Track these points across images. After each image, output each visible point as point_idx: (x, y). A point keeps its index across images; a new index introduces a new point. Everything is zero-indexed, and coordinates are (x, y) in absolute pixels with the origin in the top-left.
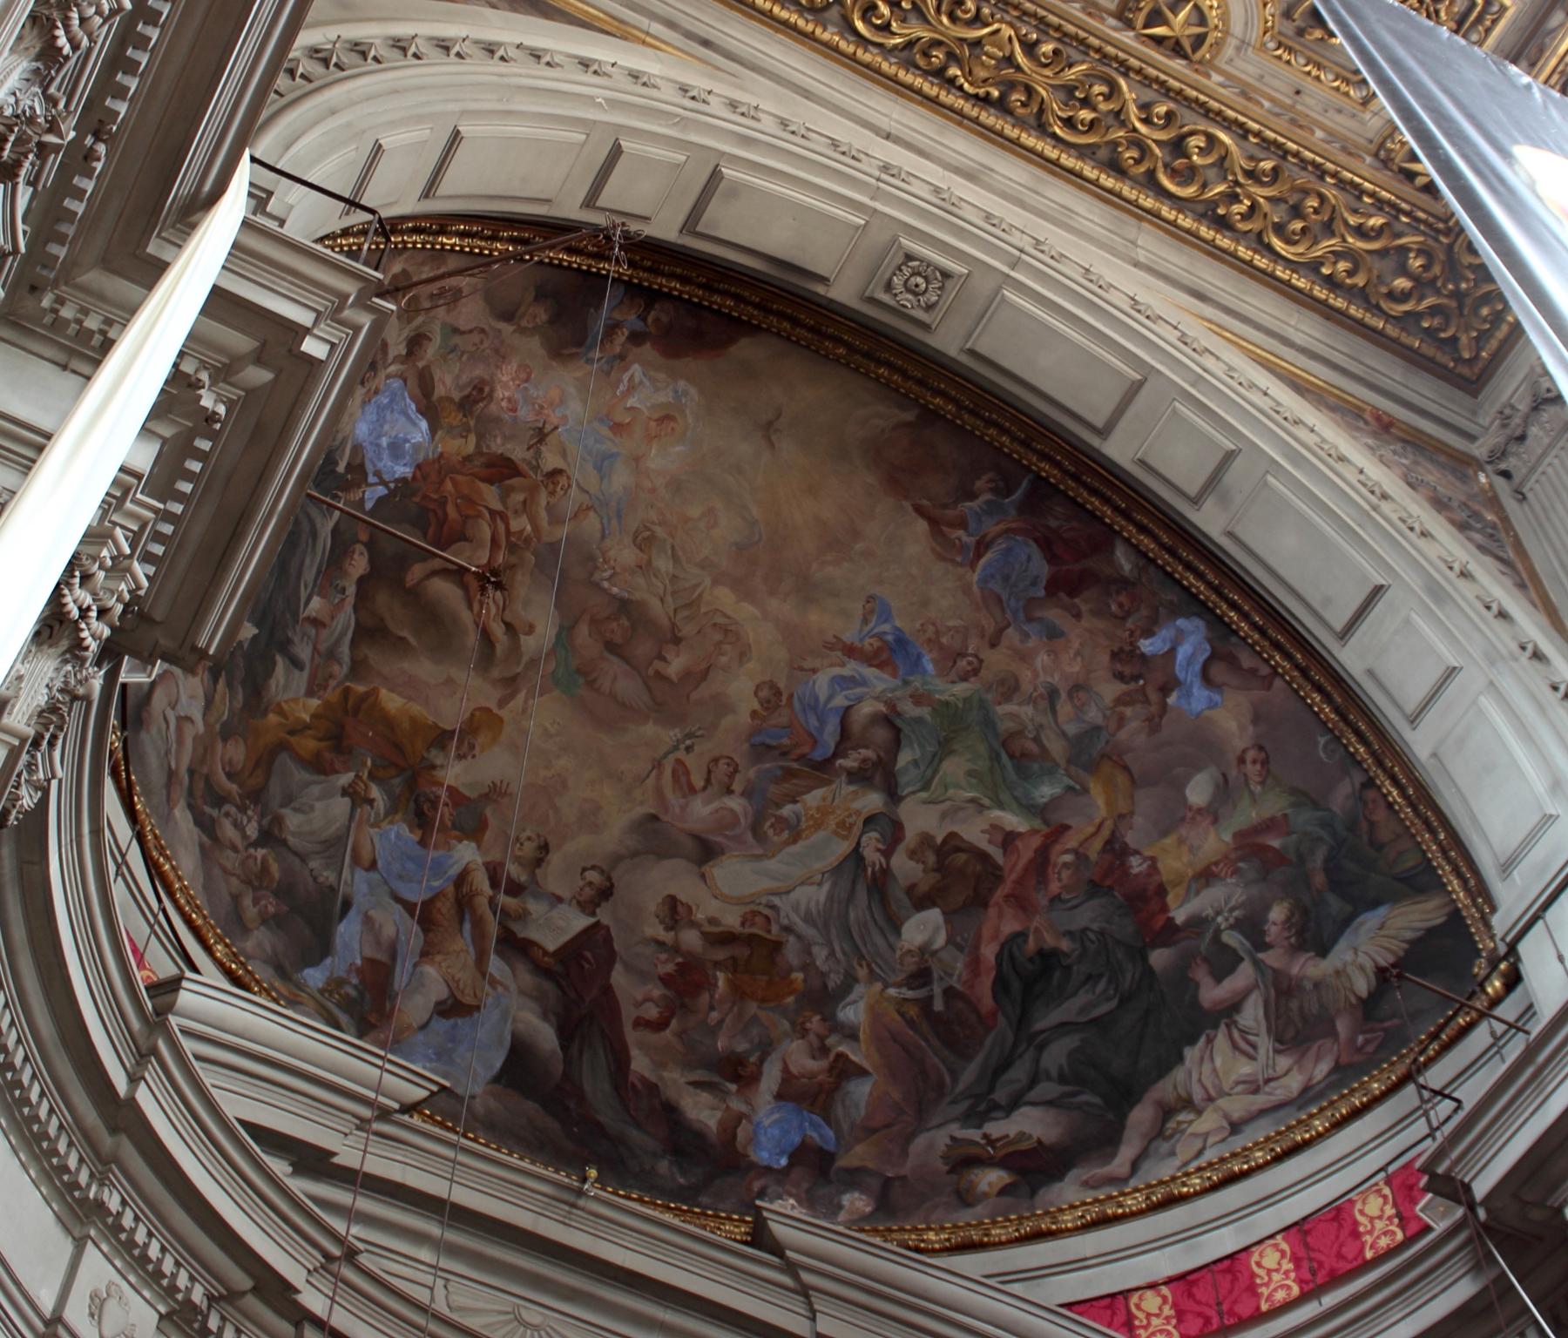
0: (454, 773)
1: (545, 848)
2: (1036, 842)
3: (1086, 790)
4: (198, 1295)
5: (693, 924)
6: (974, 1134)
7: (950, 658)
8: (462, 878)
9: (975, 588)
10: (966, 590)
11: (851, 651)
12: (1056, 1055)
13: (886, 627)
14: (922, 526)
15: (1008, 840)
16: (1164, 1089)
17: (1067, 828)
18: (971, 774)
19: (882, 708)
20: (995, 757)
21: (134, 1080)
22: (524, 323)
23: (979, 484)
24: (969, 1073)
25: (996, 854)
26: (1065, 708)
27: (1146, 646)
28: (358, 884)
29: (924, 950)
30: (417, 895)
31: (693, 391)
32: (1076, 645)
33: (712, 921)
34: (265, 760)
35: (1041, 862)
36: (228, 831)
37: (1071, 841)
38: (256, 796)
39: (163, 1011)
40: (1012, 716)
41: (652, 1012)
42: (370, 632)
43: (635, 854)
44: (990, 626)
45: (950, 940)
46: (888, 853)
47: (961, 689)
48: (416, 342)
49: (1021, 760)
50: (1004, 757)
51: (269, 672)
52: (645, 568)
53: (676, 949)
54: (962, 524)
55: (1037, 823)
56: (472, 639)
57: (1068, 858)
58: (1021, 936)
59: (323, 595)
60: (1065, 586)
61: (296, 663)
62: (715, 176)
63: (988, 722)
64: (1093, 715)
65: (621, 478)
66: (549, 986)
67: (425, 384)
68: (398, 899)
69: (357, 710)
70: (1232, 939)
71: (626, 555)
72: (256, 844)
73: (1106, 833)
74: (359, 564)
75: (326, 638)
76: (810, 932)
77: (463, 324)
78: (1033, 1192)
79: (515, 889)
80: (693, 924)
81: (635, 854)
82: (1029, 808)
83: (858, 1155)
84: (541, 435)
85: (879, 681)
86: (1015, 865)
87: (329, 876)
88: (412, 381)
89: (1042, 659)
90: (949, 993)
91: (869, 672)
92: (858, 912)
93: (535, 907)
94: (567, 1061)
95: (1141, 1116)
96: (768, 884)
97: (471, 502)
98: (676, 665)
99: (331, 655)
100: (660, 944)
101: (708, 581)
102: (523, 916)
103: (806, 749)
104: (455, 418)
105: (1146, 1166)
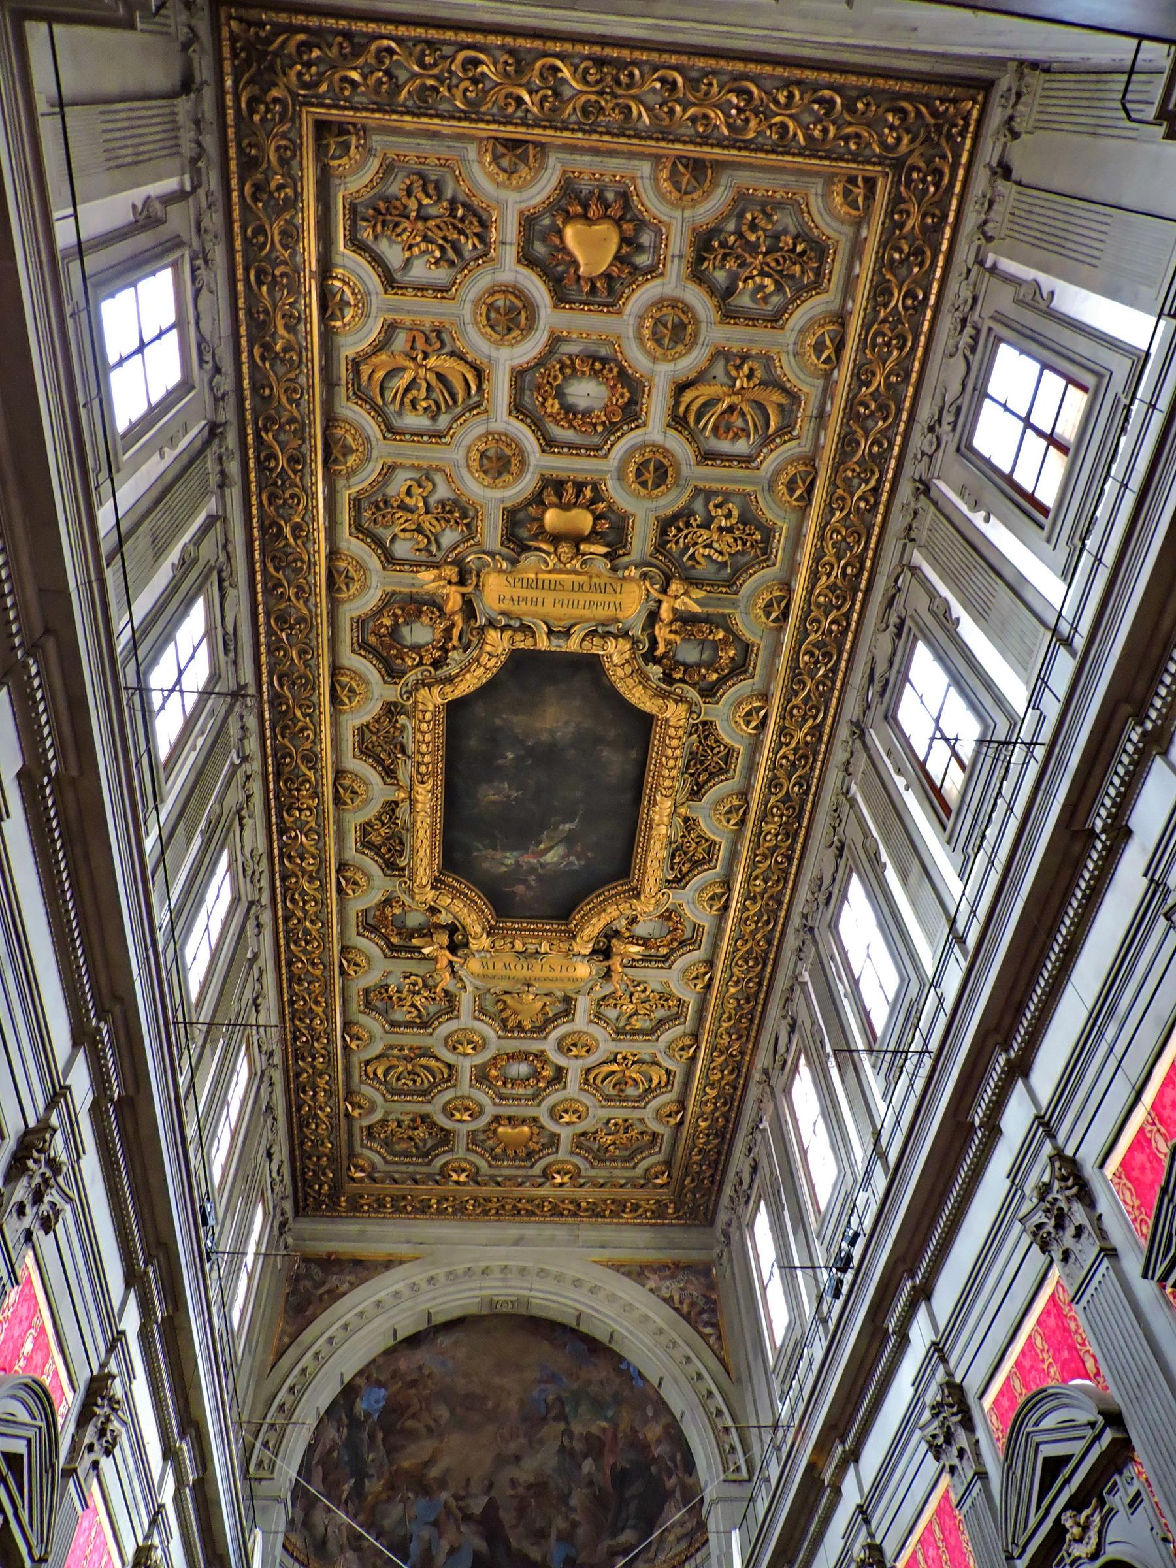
0: (434, 1472)
1: (468, 1480)
6: (612, 1542)
12: (633, 1507)
15: (604, 1430)
24: (610, 1516)
28: (412, 1528)
30: (432, 1519)
37: (622, 1427)
42: (392, 1450)
56: (424, 1431)
58: (614, 1464)
71: (462, 1382)
74: (380, 1435)
79: (463, 1498)
82: (606, 1419)
84: (420, 1368)
86: (608, 1439)
87: (402, 1532)
93: (471, 1501)
98: (490, 1404)
99: (381, 1465)
102: (468, 1506)
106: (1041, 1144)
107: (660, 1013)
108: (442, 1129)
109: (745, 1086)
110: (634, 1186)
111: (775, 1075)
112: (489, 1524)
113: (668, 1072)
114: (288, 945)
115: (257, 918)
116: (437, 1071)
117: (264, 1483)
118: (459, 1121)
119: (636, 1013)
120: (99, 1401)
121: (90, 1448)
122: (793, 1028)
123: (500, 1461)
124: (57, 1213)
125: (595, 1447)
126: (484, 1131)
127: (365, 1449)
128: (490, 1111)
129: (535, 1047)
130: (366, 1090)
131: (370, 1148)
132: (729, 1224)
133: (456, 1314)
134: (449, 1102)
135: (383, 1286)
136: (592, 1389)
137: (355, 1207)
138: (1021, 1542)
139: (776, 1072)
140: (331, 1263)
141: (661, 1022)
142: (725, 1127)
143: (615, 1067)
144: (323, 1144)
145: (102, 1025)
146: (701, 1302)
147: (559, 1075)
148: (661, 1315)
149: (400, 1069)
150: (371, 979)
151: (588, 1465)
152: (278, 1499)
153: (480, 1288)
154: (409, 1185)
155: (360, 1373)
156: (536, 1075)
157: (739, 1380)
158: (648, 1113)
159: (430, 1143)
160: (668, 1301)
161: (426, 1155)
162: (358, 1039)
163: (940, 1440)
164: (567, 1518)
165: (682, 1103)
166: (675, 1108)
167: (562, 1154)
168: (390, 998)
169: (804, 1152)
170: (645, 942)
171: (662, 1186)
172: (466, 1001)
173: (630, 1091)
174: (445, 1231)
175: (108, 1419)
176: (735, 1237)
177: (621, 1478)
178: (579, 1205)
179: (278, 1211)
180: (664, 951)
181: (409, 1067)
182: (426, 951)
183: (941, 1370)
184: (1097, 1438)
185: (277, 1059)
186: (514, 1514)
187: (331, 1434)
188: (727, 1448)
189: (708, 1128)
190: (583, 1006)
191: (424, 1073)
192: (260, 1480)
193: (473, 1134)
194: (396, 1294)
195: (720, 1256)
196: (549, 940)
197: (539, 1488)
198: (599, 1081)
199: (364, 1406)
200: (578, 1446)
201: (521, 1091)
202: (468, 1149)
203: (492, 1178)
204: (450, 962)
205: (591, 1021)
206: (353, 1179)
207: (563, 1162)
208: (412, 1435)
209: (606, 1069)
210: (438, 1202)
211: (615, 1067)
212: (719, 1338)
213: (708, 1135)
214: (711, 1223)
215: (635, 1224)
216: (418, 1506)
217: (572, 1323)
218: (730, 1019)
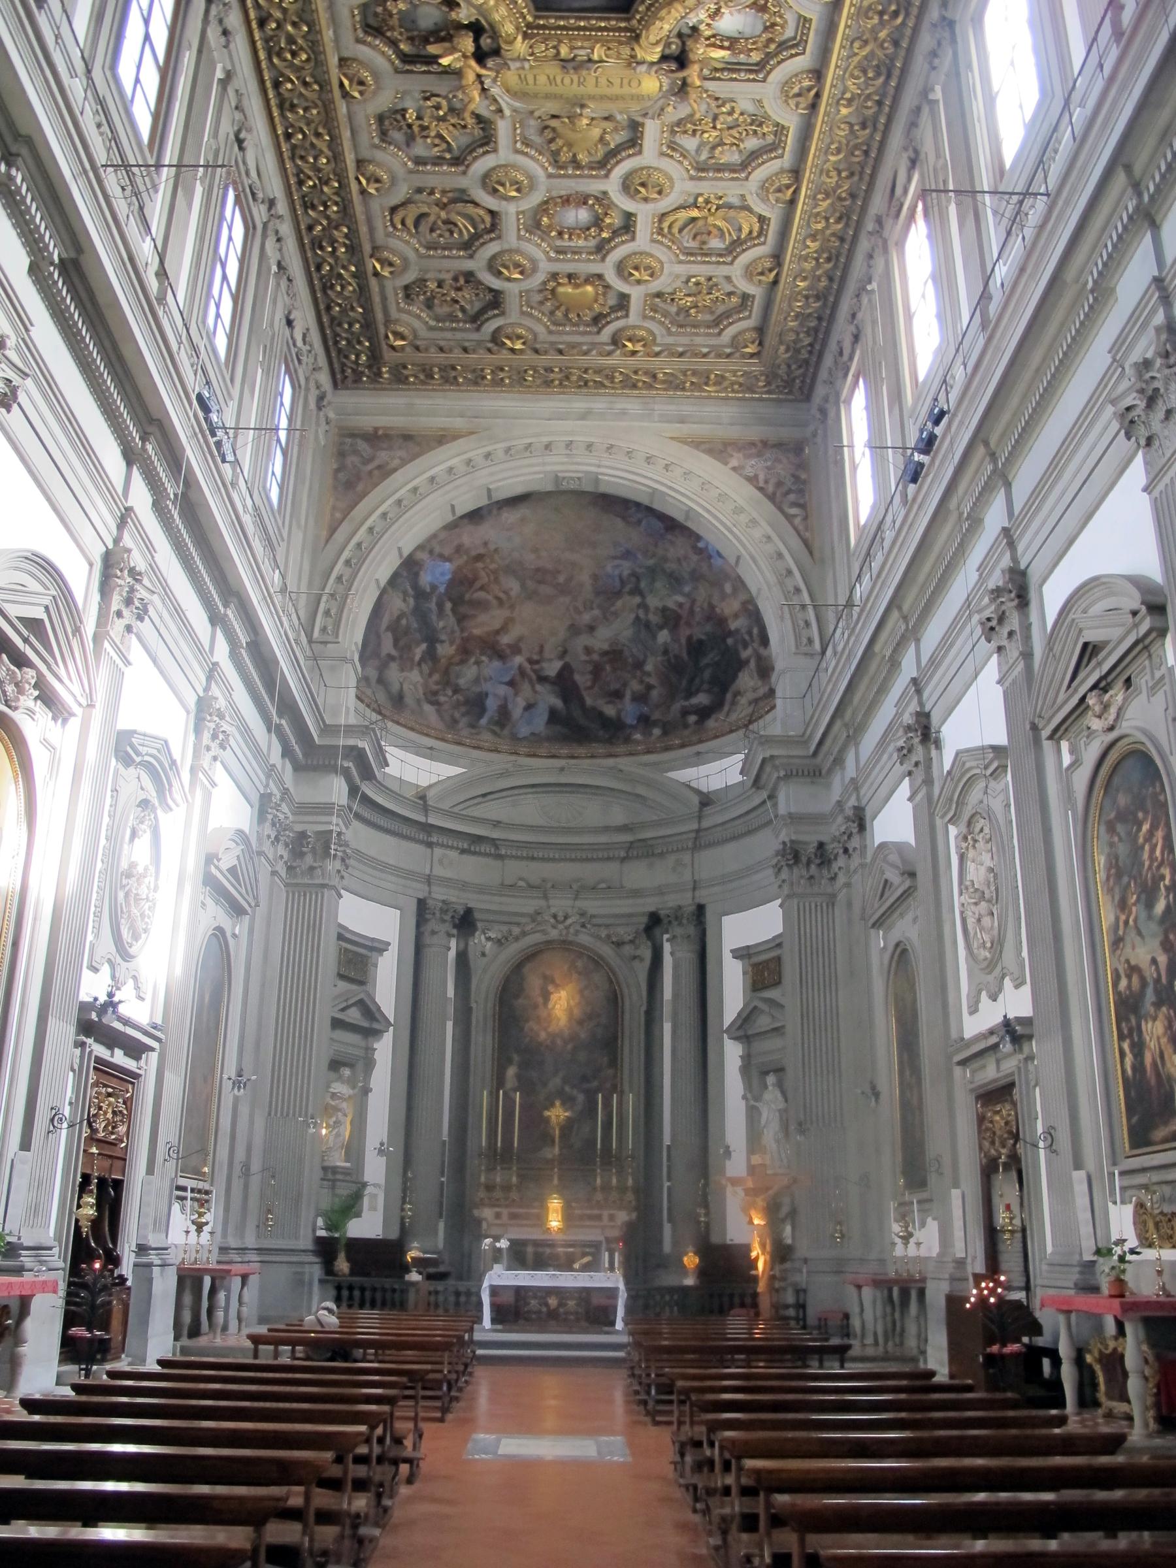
0: (505, 640)
1: (542, 647)
4: (466, 846)
6: (686, 703)
8: (520, 667)
11: (615, 558)
12: (707, 674)
15: (681, 605)
21: (426, 816)
24: (684, 683)
26: (684, 564)
28: (487, 687)
29: (665, 643)
30: (507, 679)
34: (446, 672)
35: (692, 612)
36: (442, 699)
37: (698, 604)
39: (425, 802)
41: (589, 684)
42: (461, 619)
48: (431, 552)
51: (435, 649)
56: (495, 602)
61: (442, 642)
62: (489, 490)
70: (747, 637)
71: (532, 556)
74: (448, 605)
79: (537, 662)
83: (656, 716)
84: (486, 544)
87: (478, 690)
90: (676, 657)
93: (545, 665)
95: (729, 696)
98: (561, 579)
99: (453, 632)
100: (586, 662)
102: (542, 669)
106: (1153, 311)
107: (751, 143)
108: (491, 290)
109: (855, 237)
110: (719, 356)
111: (887, 224)
112: (564, 683)
113: (762, 219)
114: (270, 59)
115: (221, 21)
116: (478, 219)
117: (329, 646)
118: (509, 279)
119: (722, 144)
120: (119, 573)
121: (119, 614)
122: (913, 162)
123: (574, 630)
124: (14, 390)
125: (671, 619)
126: (540, 291)
127: (434, 617)
128: (545, 267)
129: (594, 186)
130: (394, 243)
131: (409, 313)
132: (826, 400)
133: (519, 490)
134: (494, 258)
135: (439, 461)
136: (670, 566)
137: (399, 378)
138: (1047, 716)
139: (891, 221)
140: (376, 438)
141: (754, 155)
142: (828, 288)
143: (695, 213)
144: (353, 309)
145: (13, 172)
146: (789, 483)
147: (628, 225)
148: (742, 493)
149: (432, 218)
150: (383, 101)
151: (664, 636)
152: (344, 659)
153: (544, 464)
154: (457, 354)
155: (420, 547)
156: (597, 222)
158: (736, 271)
159: (478, 306)
160: (753, 480)
161: (477, 319)
162: (378, 181)
163: (994, 623)
164: (642, 682)
165: (777, 257)
166: (768, 265)
167: (634, 318)
168: (410, 126)
169: (909, 317)
170: (732, 43)
171: (752, 356)
172: (503, 129)
173: (715, 243)
174: (502, 403)
175: (132, 590)
176: (832, 414)
177: (696, 648)
178: (654, 376)
179: (312, 385)
180: (756, 57)
181: (443, 215)
182: (445, 61)
183: (1008, 555)
184: (1136, 625)
185: (282, 207)
186: (589, 677)
187: (398, 604)
188: (802, 624)
189: (808, 288)
190: (652, 131)
191: (460, 221)
192: (325, 643)
193: (525, 294)
194: (450, 470)
195: (815, 435)
196: (604, 42)
197: (614, 655)
198: (675, 230)
200: (654, 619)
201: (581, 243)
202: (523, 313)
203: (552, 343)
204: (479, 76)
205: (663, 154)
206: (393, 348)
207: (634, 327)
209: (683, 215)
210: (492, 372)
211: (695, 213)
212: (805, 518)
213: (807, 297)
214: (808, 398)
215: (718, 398)
216: (492, 667)
217: (645, 501)
218: (839, 151)
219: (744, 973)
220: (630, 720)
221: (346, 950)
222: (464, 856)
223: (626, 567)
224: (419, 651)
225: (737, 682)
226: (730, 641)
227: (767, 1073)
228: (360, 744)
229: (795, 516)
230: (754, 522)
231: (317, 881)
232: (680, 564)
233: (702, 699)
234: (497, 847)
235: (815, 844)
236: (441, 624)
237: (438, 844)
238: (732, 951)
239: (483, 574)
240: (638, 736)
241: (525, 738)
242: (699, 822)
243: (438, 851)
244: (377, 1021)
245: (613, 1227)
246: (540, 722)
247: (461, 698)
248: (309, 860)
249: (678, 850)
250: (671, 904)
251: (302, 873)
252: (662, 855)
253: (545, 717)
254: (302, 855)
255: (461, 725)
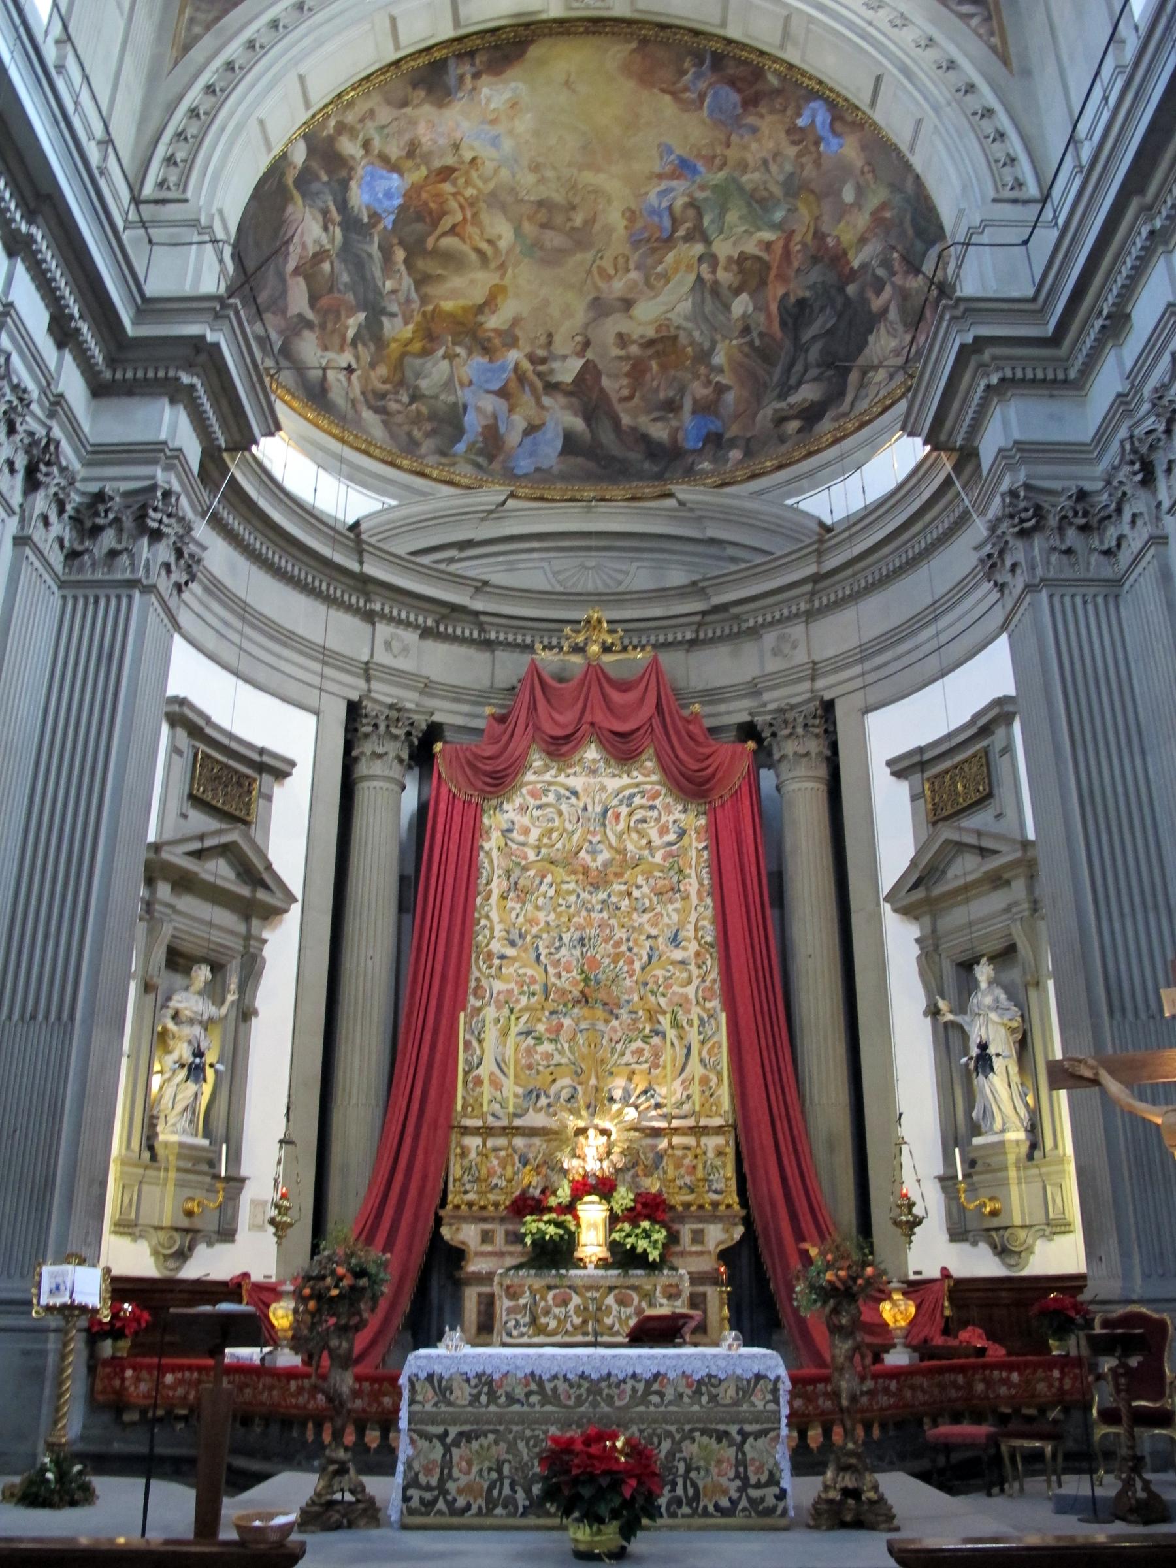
0: (494, 322)
2: (781, 243)
3: (796, 210)
5: (634, 342)
6: (783, 405)
7: (710, 160)
8: (516, 368)
9: (708, 121)
10: (703, 122)
11: (660, 177)
12: (814, 354)
13: (672, 157)
14: (667, 98)
15: (768, 246)
16: (861, 361)
17: (793, 232)
18: (740, 218)
19: (686, 199)
20: (749, 205)
22: (415, 102)
23: (686, 65)
24: (778, 372)
25: (764, 255)
26: (774, 168)
27: (801, 122)
28: (464, 395)
29: (744, 316)
30: (496, 386)
31: (521, 85)
32: (767, 132)
33: (642, 337)
36: (393, 406)
37: (797, 238)
38: (401, 383)
40: (751, 181)
41: (625, 392)
42: (422, 281)
43: (594, 320)
44: (723, 137)
45: (755, 308)
46: (714, 272)
47: (721, 175)
48: (366, 145)
49: (762, 202)
50: (755, 205)
51: (381, 324)
52: (542, 180)
53: (627, 358)
54: (686, 89)
55: (779, 233)
56: (473, 256)
57: (798, 247)
58: (786, 295)
59: (389, 278)
60: (751, 102)
61: (393, 315)
63: (741, 189)
64: (788, 168)
65: (507, 144)
66: (574, 400)
67: (384, 159)
68: (489, 392)
69: (433, 318)
70: (880, 272)
71: (531, 179)
72: (411, 403)
73: (812, 230)
74: (400, 254)
75: (401, 297)
76: (689, 325)
77: (384, 122)
78: (811, 430)
79: (543, 361)
80: (634, 342)
81: (594, 320)
82: (774, 227)
83: (733, 431)
84: (456, 147)
85: (680, 186)
86: (774, 258)
87: (451, 399)
88: (377, 162)
89: (754, 146)
90: (761, 335)
91: (674, 183)
92: (709, 307)
93: (556, 365)
94: (592, 431)
95: (853, 377)
96: (663, 308)
97: (438, 195)
99: (408, 301)
100: (620, 358)
101: (575, 172)
102: (552, 372)
103: (657, 235)
104: (409, 164)
105: (857, 404)
123: (600, 307)
136: (750, 179)
151: (741, 305)
157: (1027, 73)
192: (163, 202)
199: (366, 198)
200: (725, 277)
208: (451, 260)
216: (472, 365)
219: (914, 798)
220: (690, 442)
221: (206, 756)
222: (429, 644)
223: (680, 192)
224: (354, 323)
225: (867, 351)
226: (851, 289)
227: (976, 961)
228: (211, 337)
229: (972, 16)
230: (903, 21)
231: (118, 576)
232: (768, 170)
233: (808, 393)
234: (482, 629)
235: (1074, 490)
236: (389, 285)
237: (383, 616)
238: (889, 763)
239: (453, 204)
240: (706, 465)
241: (525, 475)
242: (819, 563)
243: (384, 630)
244: (267, 887)
245: (701, 1253)
246: (549, 451)
247: (424, 410)
248: (108, 540)
249: (780, 621)
250: (772, 706)
251: (94, 564)
252: (754, 632)
253: (559, 444)
254: (96, 531)
255: (423, 450)
